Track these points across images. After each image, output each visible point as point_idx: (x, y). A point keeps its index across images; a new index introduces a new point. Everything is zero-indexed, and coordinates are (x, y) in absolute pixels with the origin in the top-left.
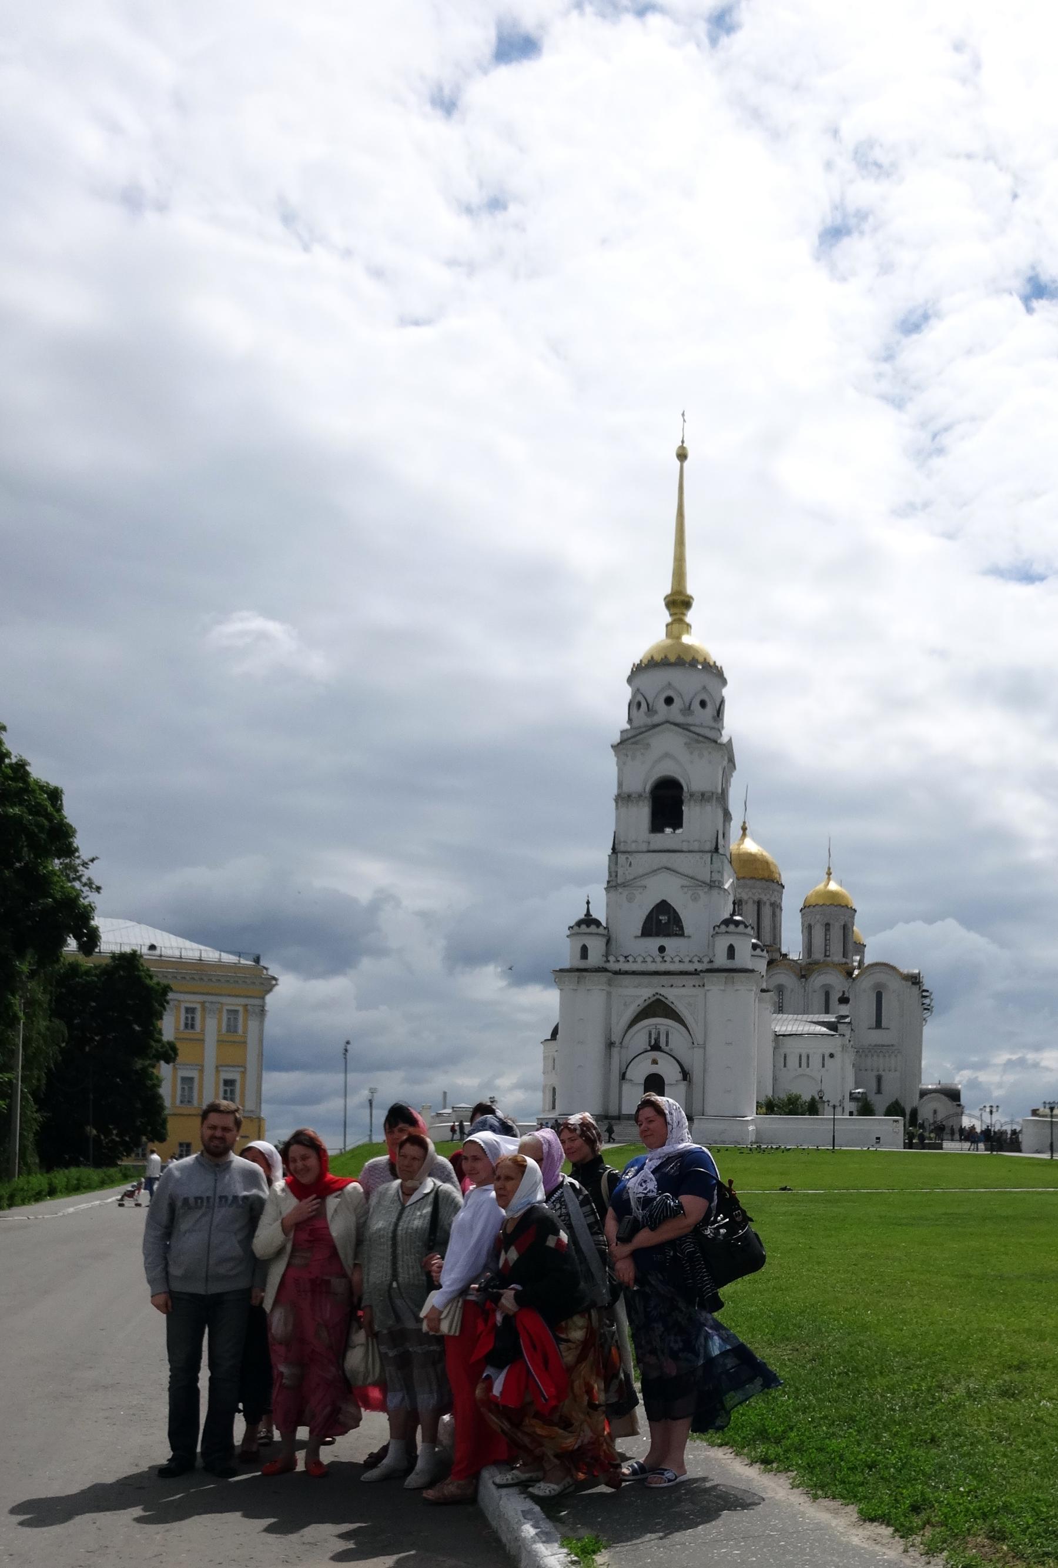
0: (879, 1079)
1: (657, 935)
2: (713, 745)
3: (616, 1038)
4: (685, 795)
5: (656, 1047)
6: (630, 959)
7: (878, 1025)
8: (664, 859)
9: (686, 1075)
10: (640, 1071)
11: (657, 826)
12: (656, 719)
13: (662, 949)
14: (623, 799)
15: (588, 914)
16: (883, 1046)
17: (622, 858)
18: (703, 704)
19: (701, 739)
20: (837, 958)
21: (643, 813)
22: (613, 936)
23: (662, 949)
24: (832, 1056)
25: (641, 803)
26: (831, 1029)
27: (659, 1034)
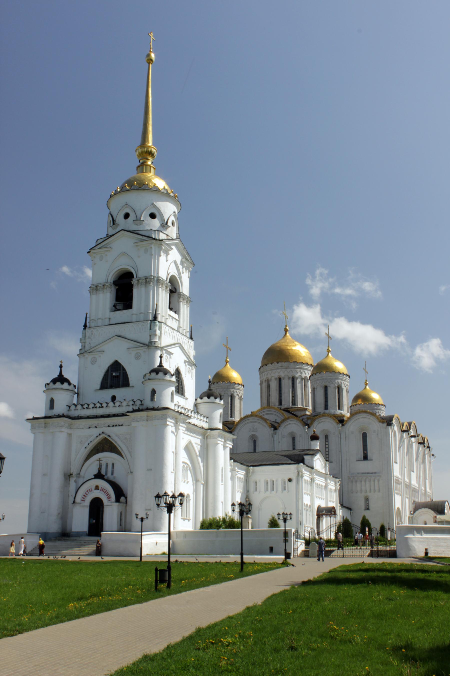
1: (111, 387)
2: (154, 241)
3: (74, 470)
4: (134, 282)
5: (99, 476)
6: (86, 406)
7: (365, 458)
8: (118, 329)
11: (115, 308)
12: (117, 230)
13: (114, 398)
15: (61, 375)
16: (368, 473)
18: (153, 216)
19: (145, 238)
21: (107, 297)
22: (81, 391)
23: (114, 398)
24: (290, 480)
25: (105, 290)
26: (292, 460)
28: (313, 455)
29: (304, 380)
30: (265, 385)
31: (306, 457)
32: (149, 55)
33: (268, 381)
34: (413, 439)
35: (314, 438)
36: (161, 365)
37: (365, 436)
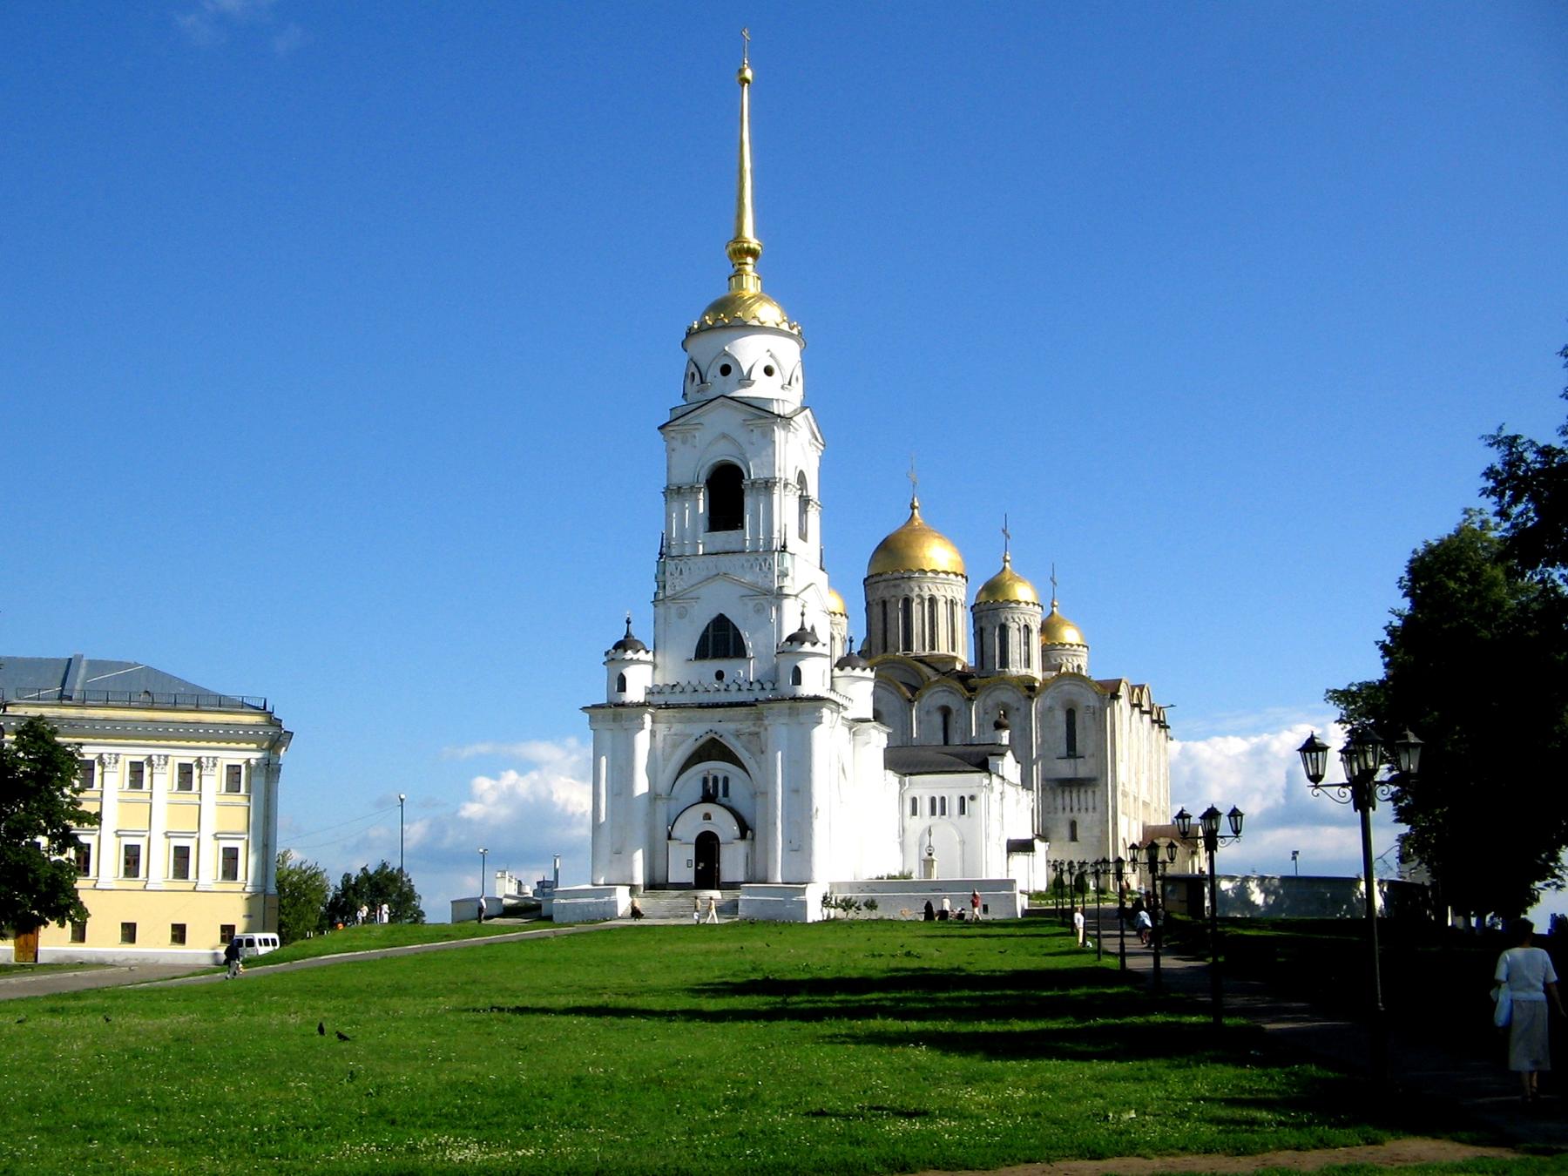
0: (1073, 825)
1: (715, 656)
5: (708, 797)
6: (678, 689)
7: (1072, 751)
9: (745, 829)
10: (690, 827)
12: (711, 394)
14: (674, 492)
17: (671, 565)
18: (769, 371)
20: (1016, 669)
24: (972, 798)
27: (715, 779)
28: (1003, 755)
29: (952, 603)
30: (878, 610)
31: (991, 759)
32: (741, 71)
33: (884, 603)
34: (1147, 717)
35: (999, 726)
36: (802, 628)
37: (1071, 714)
